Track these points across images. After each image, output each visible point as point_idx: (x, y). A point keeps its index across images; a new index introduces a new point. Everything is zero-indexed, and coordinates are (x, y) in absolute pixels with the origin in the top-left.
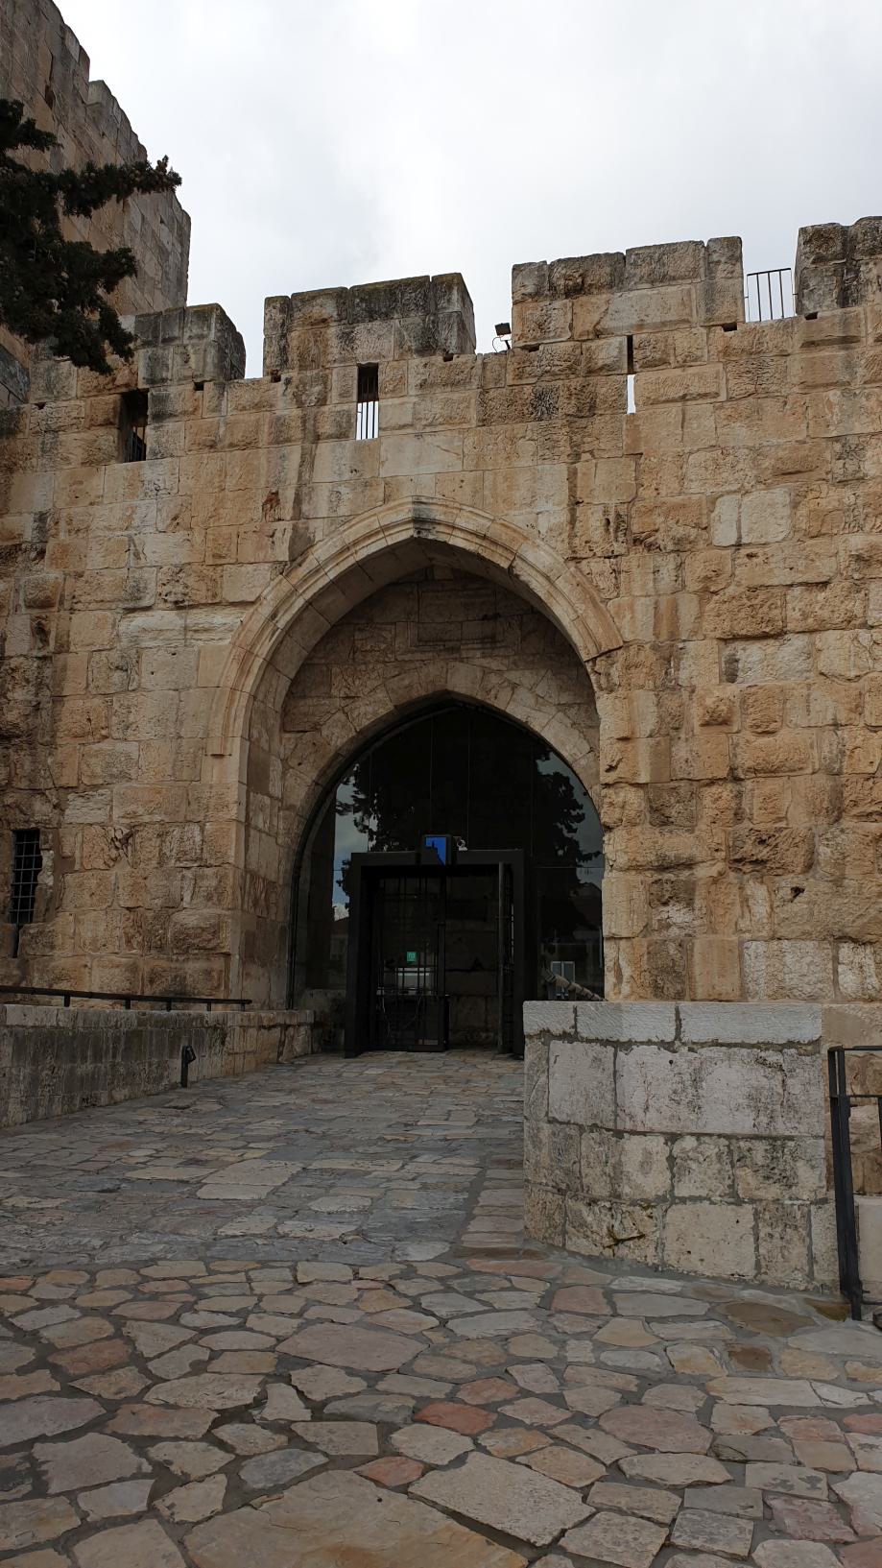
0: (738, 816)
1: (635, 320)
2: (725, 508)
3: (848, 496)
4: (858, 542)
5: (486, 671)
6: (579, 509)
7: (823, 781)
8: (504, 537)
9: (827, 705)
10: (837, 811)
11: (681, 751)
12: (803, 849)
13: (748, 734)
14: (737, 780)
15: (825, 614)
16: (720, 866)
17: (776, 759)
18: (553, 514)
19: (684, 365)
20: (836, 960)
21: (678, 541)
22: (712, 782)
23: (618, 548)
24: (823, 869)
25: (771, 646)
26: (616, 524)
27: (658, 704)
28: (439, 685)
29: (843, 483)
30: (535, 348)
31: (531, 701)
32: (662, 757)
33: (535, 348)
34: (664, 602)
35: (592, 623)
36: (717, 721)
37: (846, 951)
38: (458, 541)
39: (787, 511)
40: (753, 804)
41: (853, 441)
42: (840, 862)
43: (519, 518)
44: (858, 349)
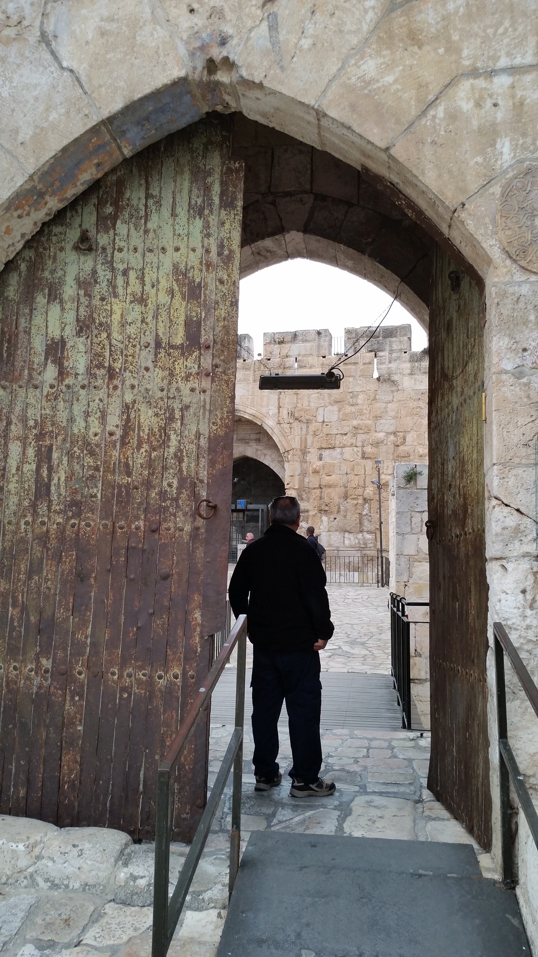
0: (321, 498)
1: (297, 353)
2: (321, 410)
3: (353, 409)
4: (355, 423)
5: (257, 450)
6: (281, 409)
7: (342, 488)
8: (260, 416)
9: (345, 468)
10: (346, 497)
11: (306, 480)
12: (337, 507)
13: (324, 476)
14: (321, 488)
15: (346, 442)
16: (315, 512)
17: (331, 483)
18: (273, 410)
19: (310, 368)
20: (344, 537)
21: (307, 420)
22: (314, 489)
23: (291, 421)
24: (342, 513)
25: (331, 451)
26: (291, 414)
27: (301, 467)
28: (243, 454)
29: (352, 405)
30: (269, 360)
31: (270, 459)
32: (302, 481)
33: (269, 360)
34: (303, 438)
35: (283, 443)
36: (316, 472)
37: (347, 535)
38: (247, 416)
39: (337, 413)
40: (325, 495)
41: (355, 393)
42: (346, 511)
43: (264, 410)
44: (358, 366)
